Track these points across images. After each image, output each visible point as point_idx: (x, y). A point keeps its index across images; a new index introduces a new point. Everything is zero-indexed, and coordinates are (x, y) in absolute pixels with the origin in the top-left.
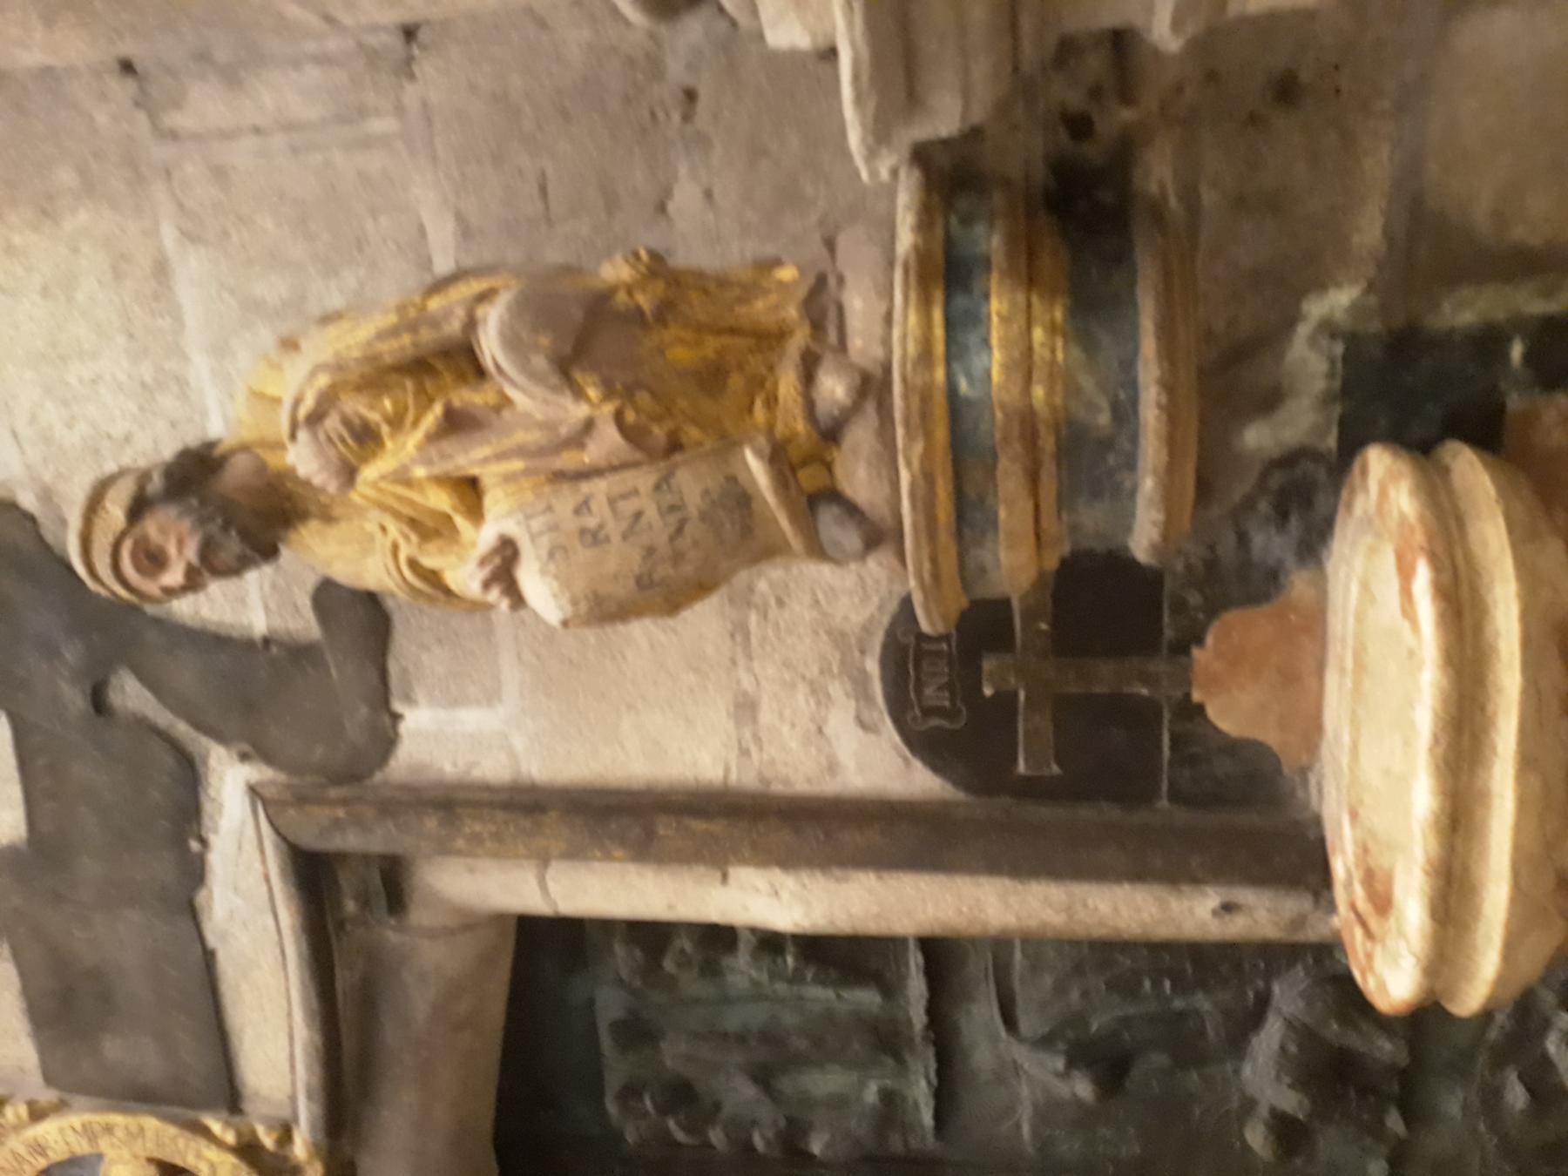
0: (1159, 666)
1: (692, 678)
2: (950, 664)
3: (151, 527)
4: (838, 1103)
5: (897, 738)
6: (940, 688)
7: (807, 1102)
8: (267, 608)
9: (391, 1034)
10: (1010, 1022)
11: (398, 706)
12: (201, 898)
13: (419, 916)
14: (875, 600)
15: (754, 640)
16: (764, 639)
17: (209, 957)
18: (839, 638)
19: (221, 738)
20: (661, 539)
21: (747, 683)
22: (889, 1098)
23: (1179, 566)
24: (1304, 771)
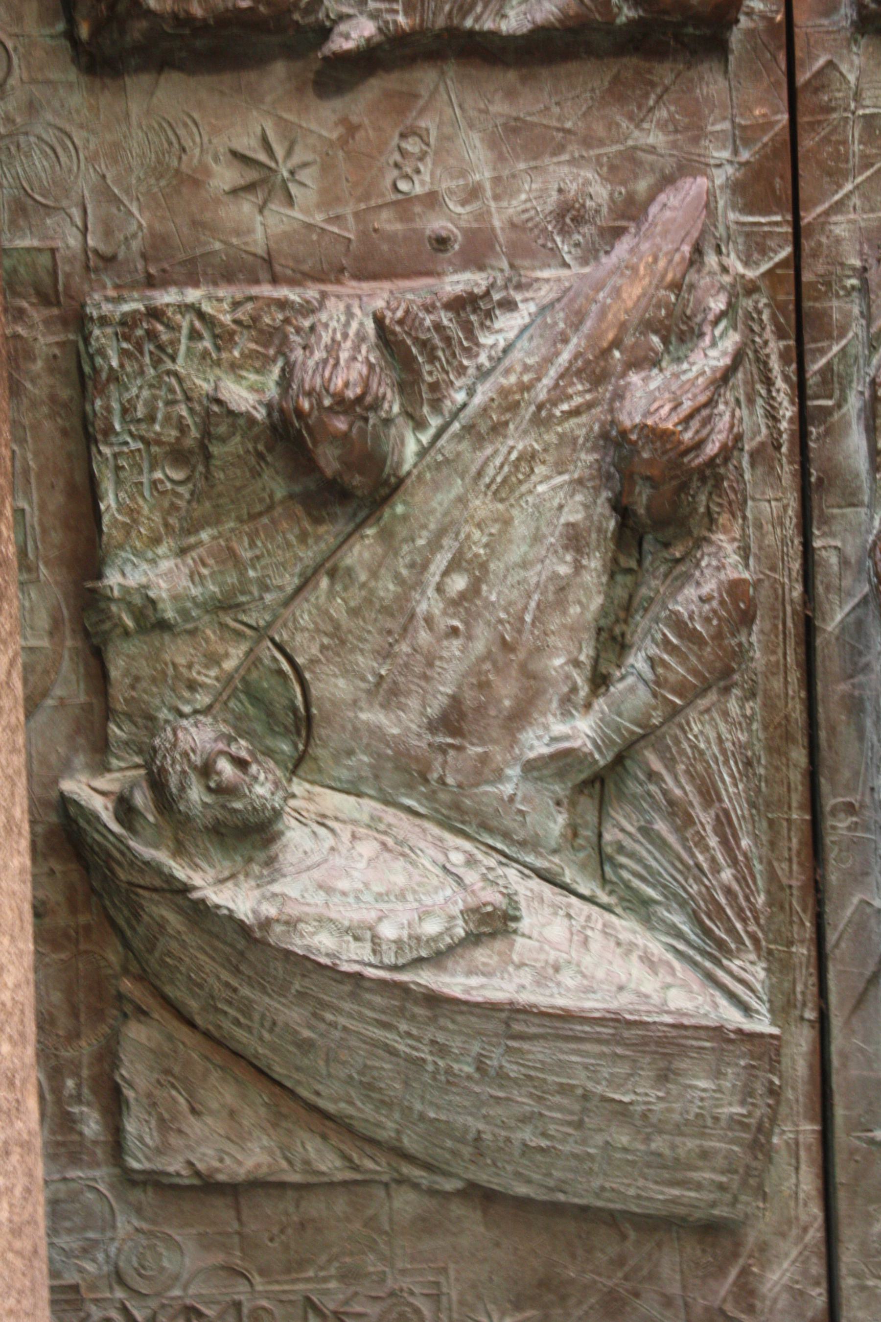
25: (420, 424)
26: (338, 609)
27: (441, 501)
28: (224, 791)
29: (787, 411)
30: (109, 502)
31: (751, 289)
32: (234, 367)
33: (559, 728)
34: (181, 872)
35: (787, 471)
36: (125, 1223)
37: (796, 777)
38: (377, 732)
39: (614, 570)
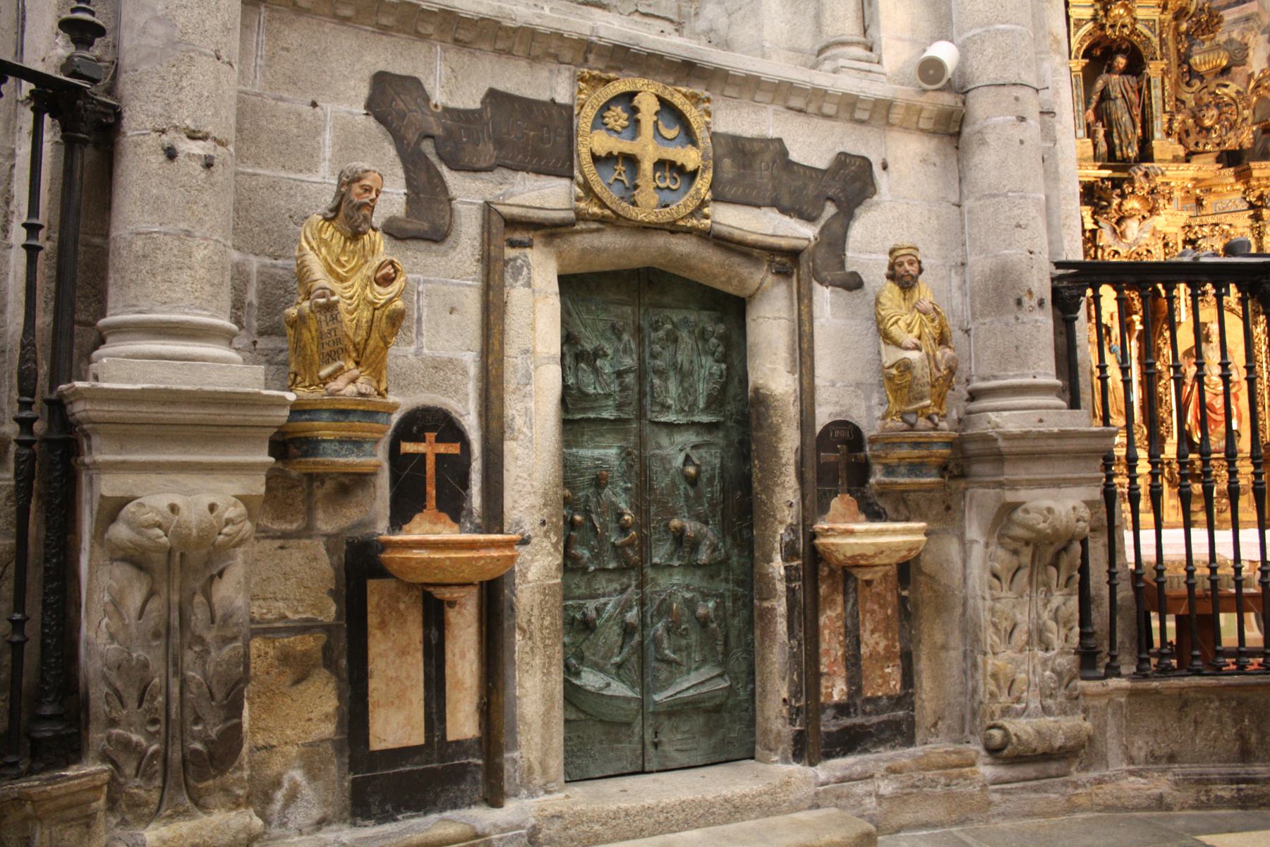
0: (845, 487)
3: (916, 265)
4: (667, 391)
9: (737, 260)
11: (830, 288)
12: (775, 210)
13: (770, 279)
17: (759, 206)
18: (848, 410)
19: (822, 232)
20: (921, 382)
21: (838, 385)
22: (669, 407)
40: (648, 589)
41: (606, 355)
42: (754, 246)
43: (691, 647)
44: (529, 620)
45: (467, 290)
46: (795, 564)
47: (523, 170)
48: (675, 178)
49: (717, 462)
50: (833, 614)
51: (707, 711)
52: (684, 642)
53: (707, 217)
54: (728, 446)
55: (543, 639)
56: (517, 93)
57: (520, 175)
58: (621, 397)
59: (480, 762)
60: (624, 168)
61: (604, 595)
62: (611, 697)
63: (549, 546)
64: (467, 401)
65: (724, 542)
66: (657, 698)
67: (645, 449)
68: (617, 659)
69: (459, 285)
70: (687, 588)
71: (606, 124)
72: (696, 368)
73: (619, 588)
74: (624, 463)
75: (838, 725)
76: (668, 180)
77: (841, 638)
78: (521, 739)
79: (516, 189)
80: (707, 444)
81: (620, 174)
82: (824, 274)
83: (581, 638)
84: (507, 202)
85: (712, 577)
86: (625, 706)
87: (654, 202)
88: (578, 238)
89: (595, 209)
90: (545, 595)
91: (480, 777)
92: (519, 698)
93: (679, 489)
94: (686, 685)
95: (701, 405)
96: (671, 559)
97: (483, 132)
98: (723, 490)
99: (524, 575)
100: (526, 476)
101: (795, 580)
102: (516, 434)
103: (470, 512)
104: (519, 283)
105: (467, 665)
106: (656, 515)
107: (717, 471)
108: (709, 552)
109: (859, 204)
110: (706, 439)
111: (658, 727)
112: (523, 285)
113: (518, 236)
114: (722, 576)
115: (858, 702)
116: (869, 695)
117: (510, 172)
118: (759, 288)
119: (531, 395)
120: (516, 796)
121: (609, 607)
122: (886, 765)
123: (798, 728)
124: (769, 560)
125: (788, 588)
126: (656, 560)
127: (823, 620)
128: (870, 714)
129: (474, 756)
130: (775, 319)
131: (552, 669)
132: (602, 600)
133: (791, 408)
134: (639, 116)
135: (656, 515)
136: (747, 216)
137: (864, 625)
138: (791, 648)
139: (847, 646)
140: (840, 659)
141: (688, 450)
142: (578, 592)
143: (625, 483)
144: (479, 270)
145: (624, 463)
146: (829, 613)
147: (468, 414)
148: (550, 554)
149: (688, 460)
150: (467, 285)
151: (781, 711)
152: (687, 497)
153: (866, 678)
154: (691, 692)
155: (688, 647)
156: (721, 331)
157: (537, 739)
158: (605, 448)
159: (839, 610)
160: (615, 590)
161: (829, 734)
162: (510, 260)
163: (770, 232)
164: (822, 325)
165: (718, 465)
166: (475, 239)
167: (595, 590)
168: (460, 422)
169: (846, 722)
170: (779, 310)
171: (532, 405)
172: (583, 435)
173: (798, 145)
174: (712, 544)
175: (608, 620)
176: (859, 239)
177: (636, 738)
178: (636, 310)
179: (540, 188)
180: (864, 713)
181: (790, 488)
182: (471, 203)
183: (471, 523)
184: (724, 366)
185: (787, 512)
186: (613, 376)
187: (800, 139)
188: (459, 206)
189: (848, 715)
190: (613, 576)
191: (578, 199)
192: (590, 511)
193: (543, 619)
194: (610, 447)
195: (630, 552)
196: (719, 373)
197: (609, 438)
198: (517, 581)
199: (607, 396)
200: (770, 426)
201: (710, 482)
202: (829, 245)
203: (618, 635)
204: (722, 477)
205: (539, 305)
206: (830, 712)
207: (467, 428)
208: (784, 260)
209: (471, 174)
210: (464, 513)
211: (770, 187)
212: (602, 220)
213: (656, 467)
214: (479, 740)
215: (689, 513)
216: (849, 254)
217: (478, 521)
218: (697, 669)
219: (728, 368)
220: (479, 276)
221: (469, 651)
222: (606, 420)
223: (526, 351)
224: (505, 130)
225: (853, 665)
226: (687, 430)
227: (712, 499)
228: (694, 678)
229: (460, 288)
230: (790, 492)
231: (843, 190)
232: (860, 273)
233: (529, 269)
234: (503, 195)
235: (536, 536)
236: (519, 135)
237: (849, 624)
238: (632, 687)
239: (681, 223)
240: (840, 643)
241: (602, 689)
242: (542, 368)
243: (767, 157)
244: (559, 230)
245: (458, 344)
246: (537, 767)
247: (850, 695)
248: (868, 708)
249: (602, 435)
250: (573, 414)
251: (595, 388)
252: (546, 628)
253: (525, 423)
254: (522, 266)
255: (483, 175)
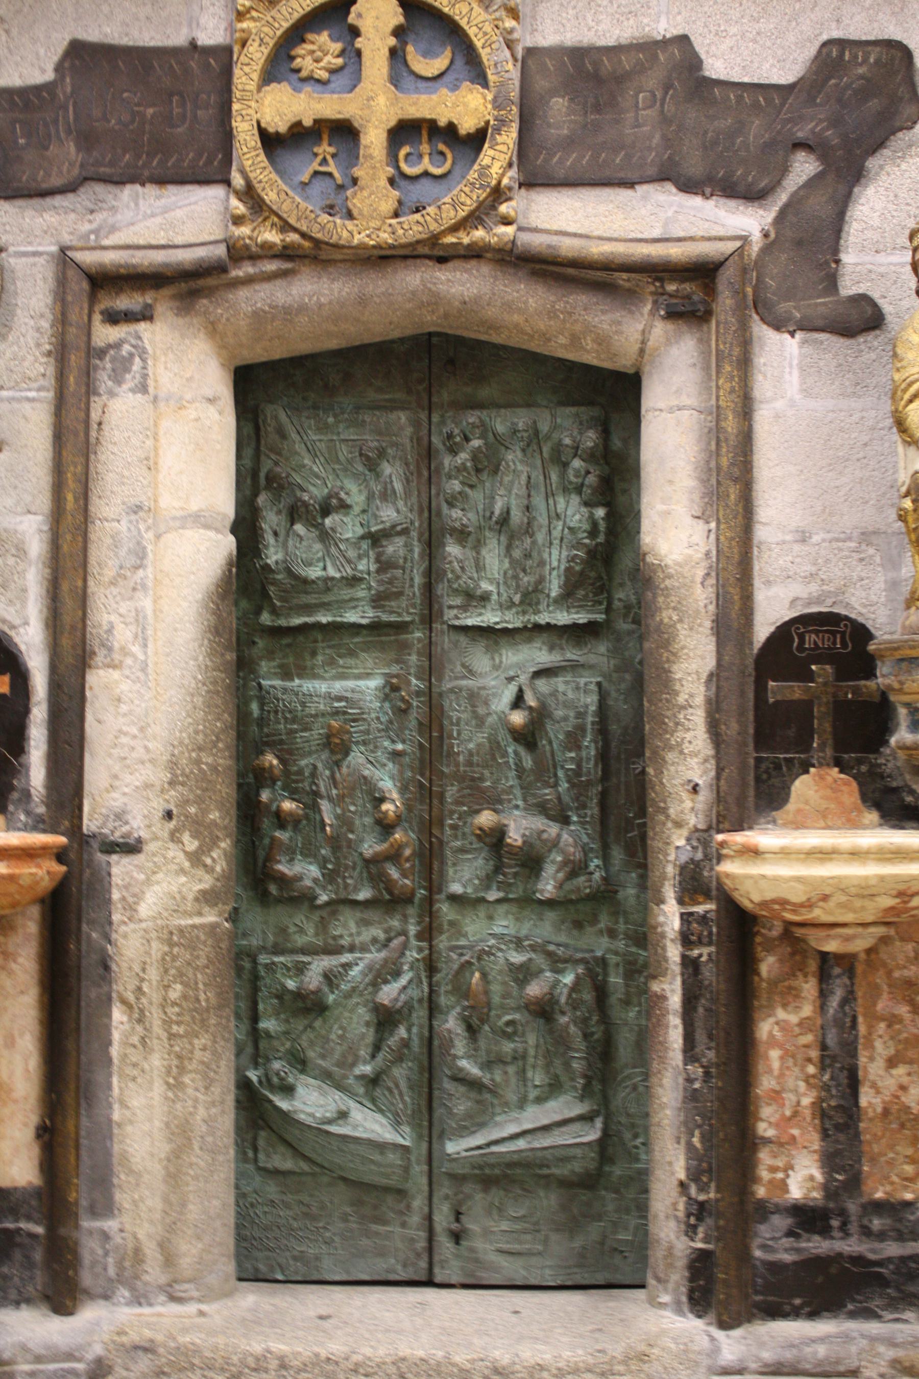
0: (829, 752)
1: (819, 509)
2: (829, 648)
4: (479, 566)
5: (787, 619)
6: (815, 643)
7: (478, 546)
8: (857, 264)
9: (580, 299)
10: (537, 674)
11: (799, 335)
12: (670, 187)
13: (660, 329)
14: (864, 611)
15: (840, 544)
16: (840, 550)
17: (630, 184)
18: (841, 591)
19: (779, 220)
21: (816, 539)
22: (485, 598)
23: (881, 761)
24: (774, 822)
25: (333, 993)
26: (312, 1036)
27: (336, 1012)
28: (282, 1079)
29: (426, 989)
30: (261, 1007)
31: (418, 960)
32: (290, 977)
33: (362, 1068)
34: (271, 1097)
35: (426, 1005)
36: (258, 1179)
37: (425, 1080)
38: (320, 1065)
39: (377, 1032)
40: (442, 942)
41: (344, 507)
42: (609, 266)
43: (524, 1057)
44: (139, 989)
45: (27, 407)
46: (700, 909)
47: (133, 180)
48: (442, 154)
49: (591, 701)
50: (794, 1019)
51: (564, 1183)
52: (508, 1047)
53: (507, 221)
54: (617, 669)
55: (167, 1023)
56: (125, 41)
57: (128, 191)
58: (381, 582)
59: (39, 1230)
60: (332, 150)
61: (352, 949)
62: (344, 1138)
63: (181, 855)
64: (24, 601)
65: (606, 857)
66: (451, 1147)
67: (440, 679)
68: (367, 1069)
69: (10, 400)
70: (518, 942)
71: (298, 71)
72: (543, 520)
73: (382, 936)
74: (387, 705)
75: (798, 1250)
76: (426, 159)
77: (811, 1069)
78: (121, 1197)
79: (120, 218)
80: (574, 667)
81: (324, 161)
82: (784, 307)
83: (299, 1024)
84: (106, 242)
85: (578, 925)
86: (377, 1157)
87: (387, 206)
88: (243, 293)
89: (271, 236)
90: (171, 945)
91: (38, 1256)
92: (119, 1125)
93: (505, 754)
94: (513, 1129)
95: (555, 588)
96: (488, 888)
97: (56, 122)
98: (604, 756)
99: (131, 908)
100: (134, 730)
101: (700, 943)
102: (117, 656)
103: (27, 795)
104: (125, 387)
105: (18, 1059)
106: (458, 803)
107: (590, 719)
108: (561, 875)
109: (881, 145)
110: (569, 656)
111: (460, 1203)
112: (132, 390)
113: (124, 302)
114: (602, 925)
115: (852, 1207)
116: (879, 1195)
117: (111, 188)
118: (642, 351)
119: (144, 587)
120: (106, 1297)
121: (355, 972)
122: (891, 1353)
123: (700, 1245)
124: (662, 901)
125: (684, 957)
126: (456, 888)
127: (765, 1029)
128: (881, 1236)
129: (29, 1218)
130: (671, 410)
131: (186, 1080)
132: (346, 958)
133: (698, 589)
134: (359, 43)
135: (458, 803)
136: (602, 208)
137: (870, 1045)
138: (689, 1080)
139: (826, 1087)
140: (807, 1113)
141: (524, 679)
142: (300, 941)
143: (393, 742)
144: (51, 371)
145: (387, 705)
146: (781, 1014)
147: (26, 623)
148: (182, 871)
149: (518, 702)
150: (29, 400)
151: (675, 1205)
152: (520, 771)
153: (873, 1160)
154: (521, 1144)
155: (519, 1057)
156: (590, 444)
157: (156, 1203)
158: (358, 677)
159: (807, 1010)
160: (375, 940)
161: (775, 1267)
162: (110, 346)
163: (656, 233)
164: (777, 416)
165: (593, 708)
166: (42, 316)
167: (334, 938)
168: (10, 639)
169: (818, 1246)
170: (678, 392)
171: (147, 604)
172: (314, 654)
173: (729, 42)
174: (565, 863)
175: (348, 995)
176: (876, 222)
177: (415, 1219)
178: (423, 416)
179: (166, 210)
180: (866, 1232)
181: (694, 754)
182: (35, 254)
183: (28, 813)
184: (600, 512)
185: (688, 804)
186: (365, 545)
187: (733, 30)
188: (12, 261)
189: (825, 1231)
190: (372, 914)
191: (238, 220)
192: (316, 794)
193: (167, 987)
194: (368, 676)
195: (394, 873)
196: (586, 526)
197: (367, 660)
198: (116, 917)
199: (354, 581)
200: (659, 629)
201: (573, 740)
202: (799, 243)
203: (367, 1024)
204: (602, 729)
205: (165, 424)
206: (781, 1222)
207: (23, 648)
208: (688, 287)
209: (36, 202)
210: (15, 795)
211: (657, 139)
212: (286, 253)
213: (456, 710)
214: (37, 1193)
215: (525, 800)
216: (848, 258)
217: (41, 810)
218: (539, 1100)
219: (608, 516)
220: (50, 382)
221: (22, 1035)
222: (355, 628)
223: (137, 509)
224: (96, 113)
225: (838, 1127)
226: (529, 640)
227: (578, 772)
228: (533, 1117)
229: (16, 405)
230: (694, 762)
231: (835, 122)
232: (875, 295)
233: (144, 360)
234: (96, 232)
235: (156, 838)
236: (125, 117)
237: (832, 1039)
238: (396, 1123)
239: (450, 239)
240: (807, 1079)
241: (330, 1122)
242: (169, 538)
243: (652, 80)
244: (201, 282)
245: (9, 502)
246: (151, 1250)
247: (830, 1191)
248: (877, 1224)
249: (352, 653)
250: (288, 616)
251: (325, 569)
252: (174, 1004)
253: (136, 636)
254: (132, 355)
255: (58, 200)
